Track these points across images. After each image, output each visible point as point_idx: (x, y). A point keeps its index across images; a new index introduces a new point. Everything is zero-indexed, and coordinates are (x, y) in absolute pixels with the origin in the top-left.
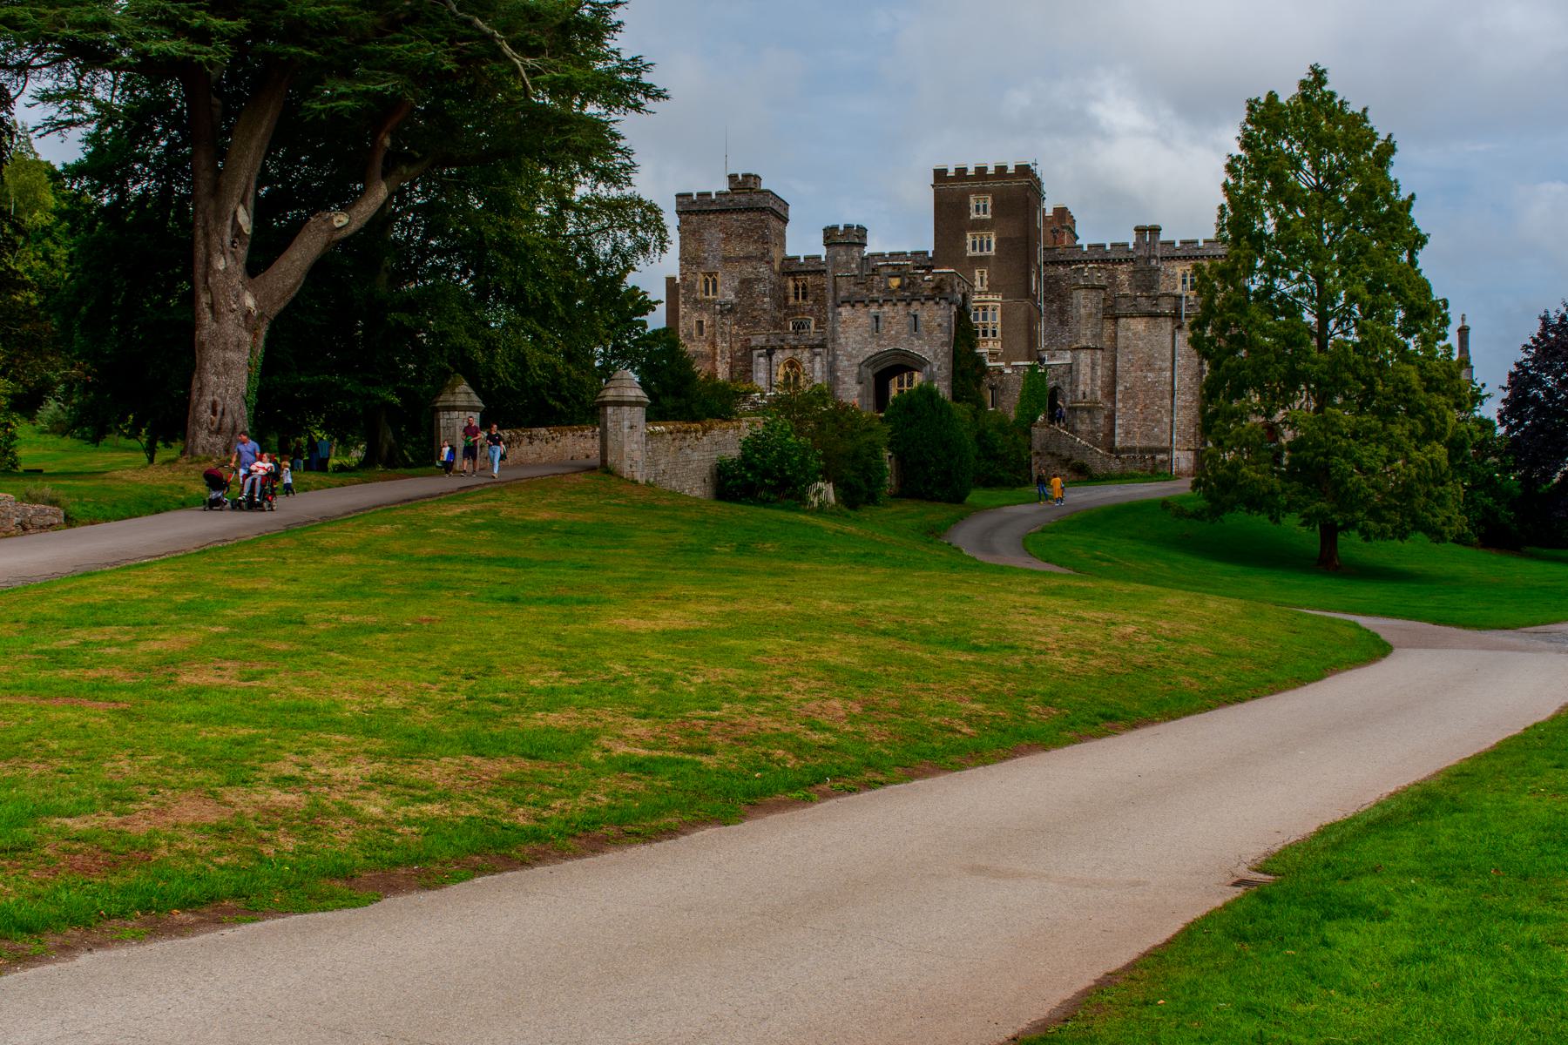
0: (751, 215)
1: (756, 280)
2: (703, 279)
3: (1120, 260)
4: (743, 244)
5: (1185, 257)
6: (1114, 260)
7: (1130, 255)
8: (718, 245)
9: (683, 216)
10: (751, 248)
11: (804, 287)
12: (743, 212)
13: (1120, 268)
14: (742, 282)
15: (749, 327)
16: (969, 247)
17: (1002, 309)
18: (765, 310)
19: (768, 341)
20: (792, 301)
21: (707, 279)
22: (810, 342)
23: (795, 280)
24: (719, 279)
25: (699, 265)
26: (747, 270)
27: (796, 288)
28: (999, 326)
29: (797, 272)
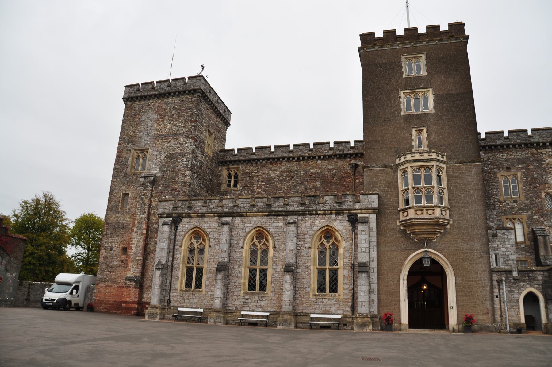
0: (184, 97)
2: (136, 155)
3: (544, 144)
6: (538, 144)
8: (152, 125)
9: (129, 103)
10: (180, 126)
11: (236, 177)
12: (178, 96)
13: (544, 151)
14: (167, 157)
16: (403, 106)
17: (447, 172)
18: (185, 183)
19: (175, 208)
20: (224, 187)
21: (139, 156)
22: (219, 210)
23: (228, 169)
24: (148, 155)
26: (174, 145)
27: (229, 176)
28: (446, 191)
29: (230, 162)
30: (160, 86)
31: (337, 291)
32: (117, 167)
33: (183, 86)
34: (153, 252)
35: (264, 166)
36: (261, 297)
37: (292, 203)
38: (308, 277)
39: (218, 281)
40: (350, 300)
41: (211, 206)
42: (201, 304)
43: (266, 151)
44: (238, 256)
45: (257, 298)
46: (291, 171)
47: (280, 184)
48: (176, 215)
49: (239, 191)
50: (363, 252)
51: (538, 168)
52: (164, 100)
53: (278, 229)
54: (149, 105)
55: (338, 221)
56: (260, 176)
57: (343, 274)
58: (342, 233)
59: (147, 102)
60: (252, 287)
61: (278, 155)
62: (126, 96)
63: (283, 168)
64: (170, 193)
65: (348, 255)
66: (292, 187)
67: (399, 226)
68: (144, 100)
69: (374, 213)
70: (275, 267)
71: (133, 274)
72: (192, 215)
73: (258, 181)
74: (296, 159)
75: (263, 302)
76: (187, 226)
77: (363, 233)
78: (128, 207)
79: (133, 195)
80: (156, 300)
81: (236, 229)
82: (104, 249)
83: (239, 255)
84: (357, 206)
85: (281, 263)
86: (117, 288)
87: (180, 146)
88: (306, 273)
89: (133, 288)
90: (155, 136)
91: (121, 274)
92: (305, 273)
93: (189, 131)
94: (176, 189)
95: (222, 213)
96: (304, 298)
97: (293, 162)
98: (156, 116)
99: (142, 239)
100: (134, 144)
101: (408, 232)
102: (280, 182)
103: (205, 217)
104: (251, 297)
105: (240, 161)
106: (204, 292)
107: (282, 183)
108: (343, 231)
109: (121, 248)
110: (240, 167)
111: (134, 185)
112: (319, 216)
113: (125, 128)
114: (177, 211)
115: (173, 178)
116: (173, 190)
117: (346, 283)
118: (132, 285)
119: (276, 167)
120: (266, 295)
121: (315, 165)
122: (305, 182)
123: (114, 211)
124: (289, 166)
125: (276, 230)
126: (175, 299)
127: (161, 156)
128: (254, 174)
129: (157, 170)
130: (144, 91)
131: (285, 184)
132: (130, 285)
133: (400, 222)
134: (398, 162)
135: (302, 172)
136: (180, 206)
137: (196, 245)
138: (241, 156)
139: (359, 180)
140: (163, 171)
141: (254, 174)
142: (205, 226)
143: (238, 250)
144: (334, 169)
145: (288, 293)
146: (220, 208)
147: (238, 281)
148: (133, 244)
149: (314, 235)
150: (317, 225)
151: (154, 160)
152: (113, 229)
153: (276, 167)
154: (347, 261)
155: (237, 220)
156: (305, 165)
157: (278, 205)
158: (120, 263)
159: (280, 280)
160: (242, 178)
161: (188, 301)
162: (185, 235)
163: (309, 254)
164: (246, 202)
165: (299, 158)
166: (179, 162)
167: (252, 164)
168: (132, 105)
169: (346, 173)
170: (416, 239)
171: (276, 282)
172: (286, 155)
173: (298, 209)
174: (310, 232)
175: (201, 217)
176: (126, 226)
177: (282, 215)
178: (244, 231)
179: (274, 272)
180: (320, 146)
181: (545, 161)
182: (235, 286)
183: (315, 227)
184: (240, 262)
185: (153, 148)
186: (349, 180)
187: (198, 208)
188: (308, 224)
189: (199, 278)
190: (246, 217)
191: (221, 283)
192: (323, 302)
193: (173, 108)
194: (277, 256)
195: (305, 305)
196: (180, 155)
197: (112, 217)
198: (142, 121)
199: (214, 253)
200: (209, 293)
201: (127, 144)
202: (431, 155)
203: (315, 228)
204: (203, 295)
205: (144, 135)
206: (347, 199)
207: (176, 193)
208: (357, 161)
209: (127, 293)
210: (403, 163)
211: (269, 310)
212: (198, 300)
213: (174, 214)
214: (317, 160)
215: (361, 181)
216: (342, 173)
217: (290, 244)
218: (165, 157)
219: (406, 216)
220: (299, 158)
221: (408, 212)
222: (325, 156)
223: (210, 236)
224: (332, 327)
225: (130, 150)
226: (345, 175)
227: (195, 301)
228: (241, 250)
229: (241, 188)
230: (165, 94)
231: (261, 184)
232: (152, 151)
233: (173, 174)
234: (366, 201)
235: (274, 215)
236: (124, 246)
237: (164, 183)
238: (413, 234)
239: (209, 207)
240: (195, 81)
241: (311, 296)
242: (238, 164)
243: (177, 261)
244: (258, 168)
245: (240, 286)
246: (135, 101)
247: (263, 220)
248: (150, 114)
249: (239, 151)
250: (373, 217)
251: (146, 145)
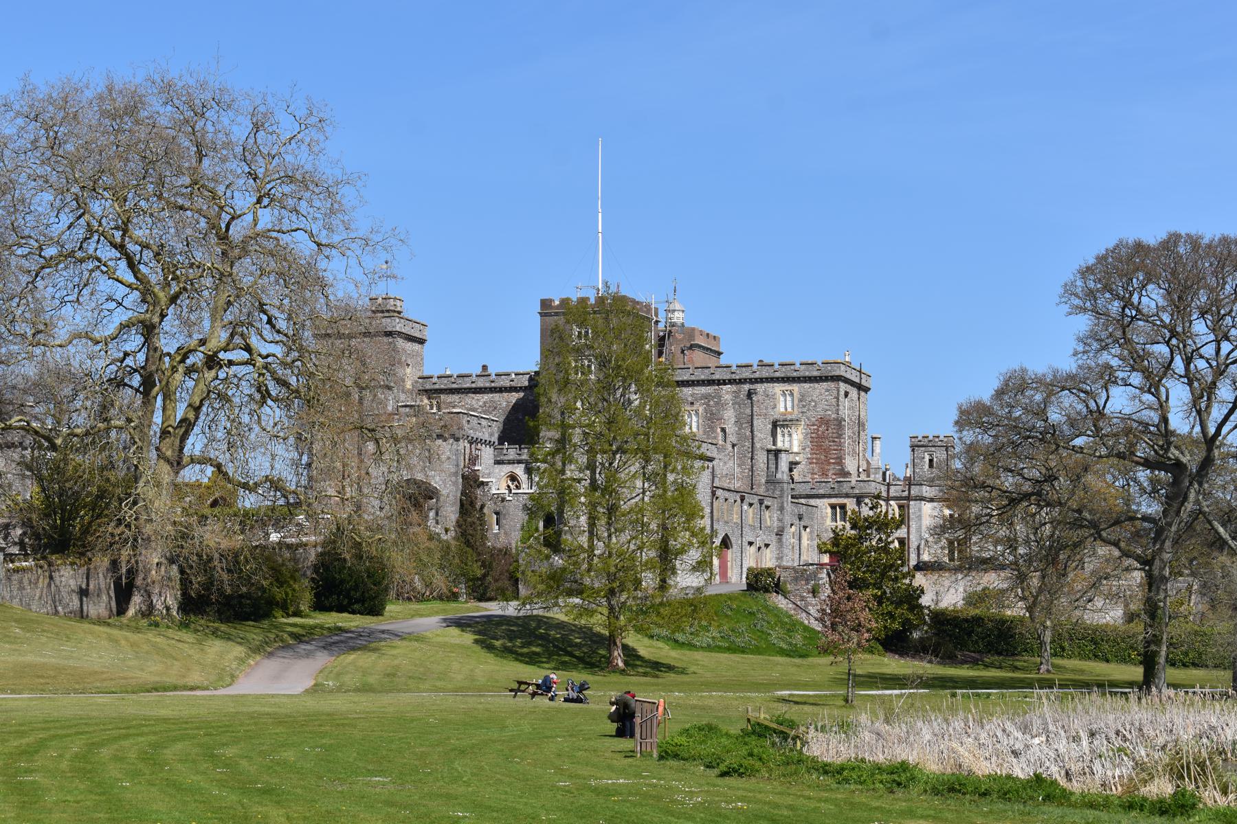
3: (724, 381)
5: (783, 378)
6: (719, 380)
7: (733, 376)
51: (717, 404)
188: (497, 471)
203: (503, 474)
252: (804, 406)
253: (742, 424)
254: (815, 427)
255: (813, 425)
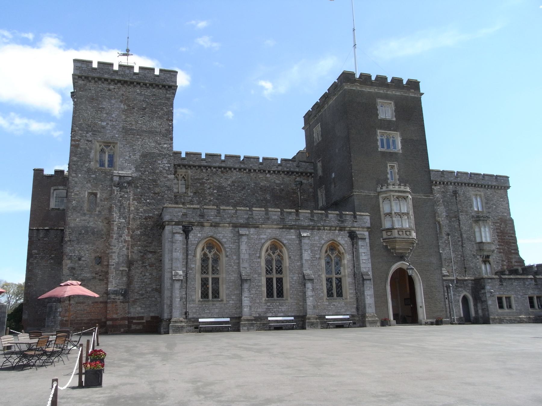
1: (159, 155)
2: (99, 149)
4: (147, 119)
9: (81, 82)
10: (155, 124)
12: (148, 88)
14: (144, 156)
15: (149, 203)
25: (95, 132)
30: (124, 72)
31: (283, 296)
32: (75, 159)
33: (154, 79)
34: (136, 262)
35: (215, 174)
36: (282, 303)
37: (302, 219)
38: (320, 284)
39: (246, 290)
40: (355, 303)
41: (226, 216)
42: (223, 313)
43: (217, 159)
44: (256, 265)
45: (278, 304)
46: (243, 182)
47: (232, 193)
48: (186, 223)
49: (190, 196)
50: (364, 263)
52: (131, 89)
53: (291, 241)
54: (109, 90)
55: (341, 236)
56: (212, 183)
57: (348, 282)
58: (345, 247)
59: (105, 85)
60: (270, 294)
61: (230, 164)
62: (78, 73)
63: (234, 178)
64: (152, 196)
65: (351, 265)
66: (244, 197)
67: (383, 243)
68: (103, 83)
69: (367, 231)
70: (292, 276)
71: (116, 287)
72: (206, 224)
73: (209, 188)
74: (247, 170)
75: (285, 307)
76: (199, 235)
77: (363, 247)
78: (98, 209)
79: (103, 195)
80: (178, 313)
81: (252, 240)
82: (69, 259)
83: (257, 264)
84: (355, 224)
85: (297, 272)
86: (93, 304)
87: (158, 146)
88: (319, 281)
89: (121, 302)
90: (123, 129)
91: (97, 288)
92: (318, 280)
93: (166, 130)
94: (158, 193)
95: (238, 224)
96: (319, 302)
97: (244, 173)
98: (122, 106)
99: (125, 247)
100: (96, 134)
101: (389, 248)
102: (232, 192)
103: (219, 226)
104: (273, 304)
105: (190, 166)
106: (225, 302)
107: (234, 193)
108: (345, 245)
109: (93, 257)
110: (189, 171)
111: (102, 183)
112: (325, 231)
113: (80, 113)
114: (187, 219)
115: (154, 181)
116: (155, 193)
117: (351, 289)
118: (119, 299)
119: (226, 176)
120: (286, 301)
121: (264, 178)
122: (256, 194)
123: (79, 212)
124: (239, 176)
125: (290, 242)
126: (194, 311)
127: (136, 154)
128: (205, 180)
129: (132, 169)
130: (102, 72)
131: (237, 194)
132: (117, 300)
133: (383, 240)
134: (379, 189)
135: (253, 184)
136: (191, 214)
137: (210, 256)
138: (191, 161)
139: (304, 197)
140: (141, 171)
141: (205, 180)
142: (219, 236)
143: (255, 260)
144: (282, 184)
145: (311, 298)
146: (235, 219)
147: (259, 289)
148: (114, 252)
149: (322, 247)
150: (324, 239)
151: (127, 158)
152: (80, 234)
153: (226, 176)
154: (350, 271)
155: (252, 230)
156: (256, 178)
157: (291, 220)
158: (94, 275)
159: (297, 288)
160: (192, 183)
161: (208, 311)
162: (198, 244)
163: (320, 264)
164: (261, 215)
165: (250, 170)
166: (159, 164)
167: (202, 170)
168: (85, 85)
169: (292, 189)
170: (395, 254)
171: (294, 289)
172: (237, 166)
173: (309, 224)
174: (319, 245)
175: (215, 226)
176: (97, 231)
177: (295, 229)
178: (260, 242)
179: (291, 280)
180: (269, 161)
181: (436, 196)
182: (256, 294)
183: (322, 241)
184: (259, 271)
185: (123, 143)
186: (295, 195)
187: (211, 218)
188: (317, 238)
189: (270, 288)
190: (260, 229)
191: (249, 292)
192: (334, 305)
193: (143, 101)
194: (293, 265)
195: (320, 308)
196: (159, 156)
197: (76, 220)
198: (104, 108)
199: (232, 263)
200: (230, 302)
201: (85, 132)
202: (406, 188)
203: (323, 242)
204: (225, 304)
205: (109, 126)
206: (347, 218)
207: (159, 197)
208: (302, 179)
209: (113, 309)
210: (385, 192)
211: (293, 314)
212: (219, 310)
213: (185, 222)
214: (266, 174)
215: (305, 197)
216: (289, 189)
217: (306, 254)
218: (141, 156)
219: (390, 235)
220: (250, 170)
221: (391, 232)
222: (274, 172)
223: (225, 246)
224: (345, 326)
225: (91, 141)
226: (292, 191)
227: (217, 311)
228: (259, 260)
229: (192, 194)
230: (132, 83)
231: (213, 191)
232: (122, 146)
233: (153, 176)
234: (362, 221)
235: (287, 228)
236: (98, 254)
237: (144, 186)
238: (392, 250)
239: (223, 217)
240: (169, 75)
241: (325, 301)
242: (186, 169)
243: (191, 272)
244: (208, 175)
245: (261, 294)
246: (90, 81)
247: (277, 232)
248: (113, 101)
249: (188, 155)
250: (366, 234)
251: (112, 137)
252: (489, 208)
253: (451, 218)
254: (498, 225)
255: (497, 223)
